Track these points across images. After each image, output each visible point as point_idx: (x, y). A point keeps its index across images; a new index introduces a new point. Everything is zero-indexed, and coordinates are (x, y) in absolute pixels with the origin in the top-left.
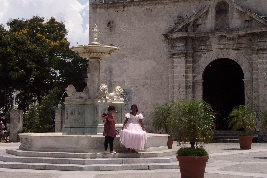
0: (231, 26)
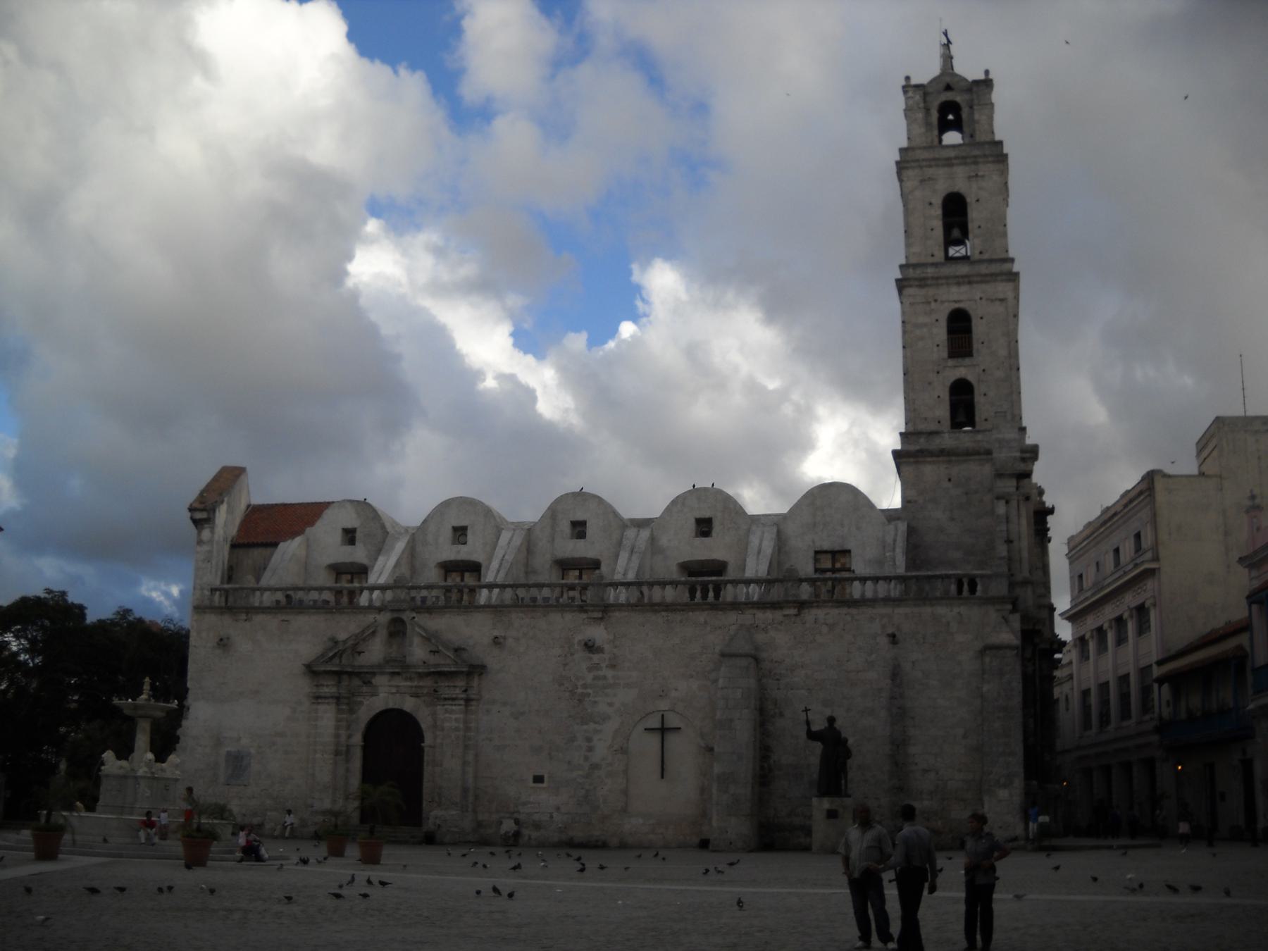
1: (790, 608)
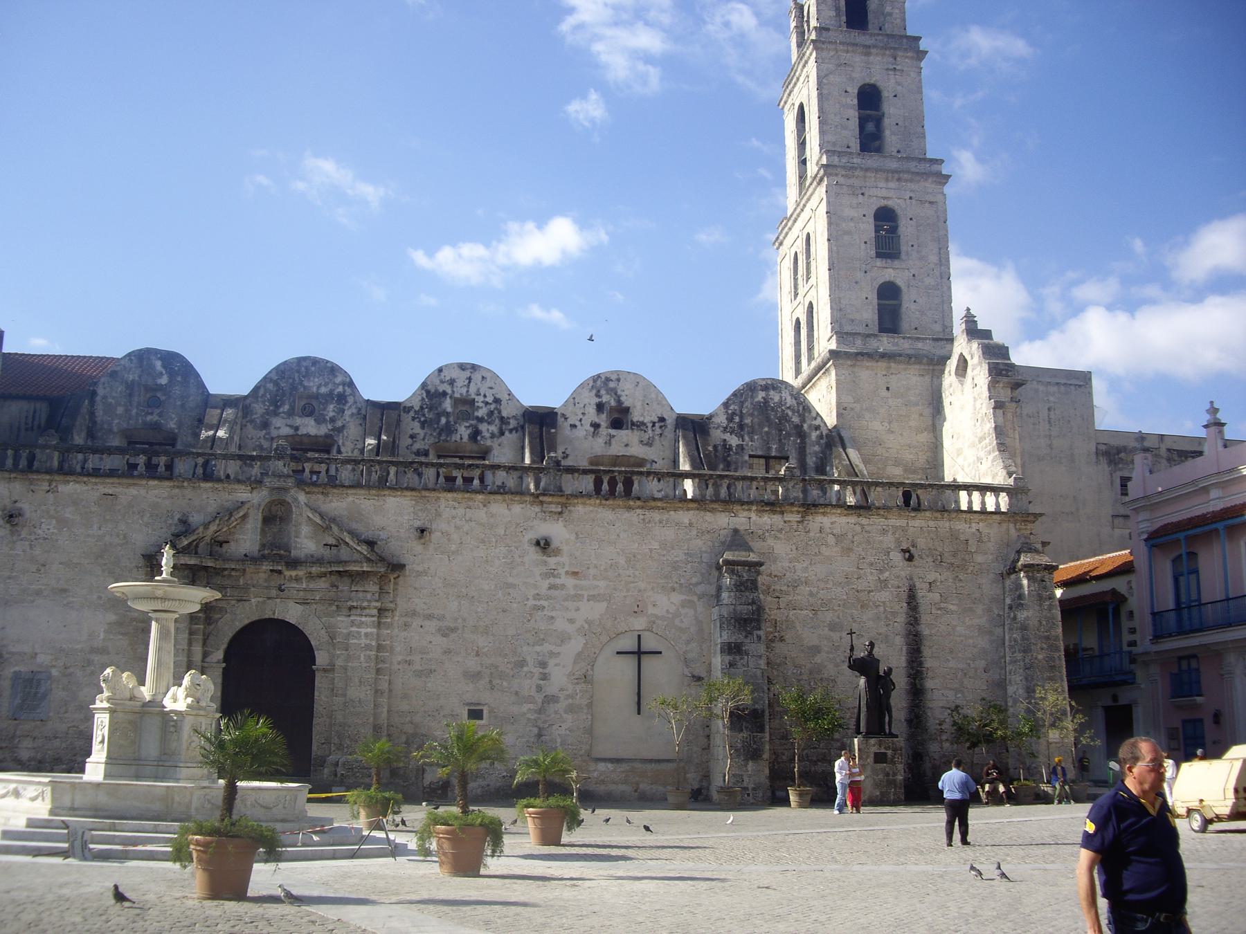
0: (293, 553)
1: (792, 512)
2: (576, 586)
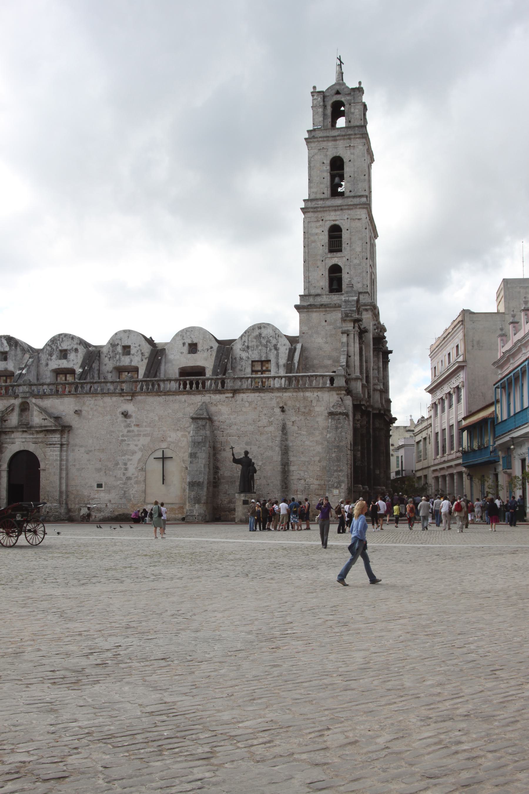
1: (228, 393)
2: (138, 431)
